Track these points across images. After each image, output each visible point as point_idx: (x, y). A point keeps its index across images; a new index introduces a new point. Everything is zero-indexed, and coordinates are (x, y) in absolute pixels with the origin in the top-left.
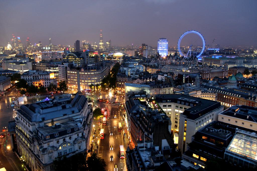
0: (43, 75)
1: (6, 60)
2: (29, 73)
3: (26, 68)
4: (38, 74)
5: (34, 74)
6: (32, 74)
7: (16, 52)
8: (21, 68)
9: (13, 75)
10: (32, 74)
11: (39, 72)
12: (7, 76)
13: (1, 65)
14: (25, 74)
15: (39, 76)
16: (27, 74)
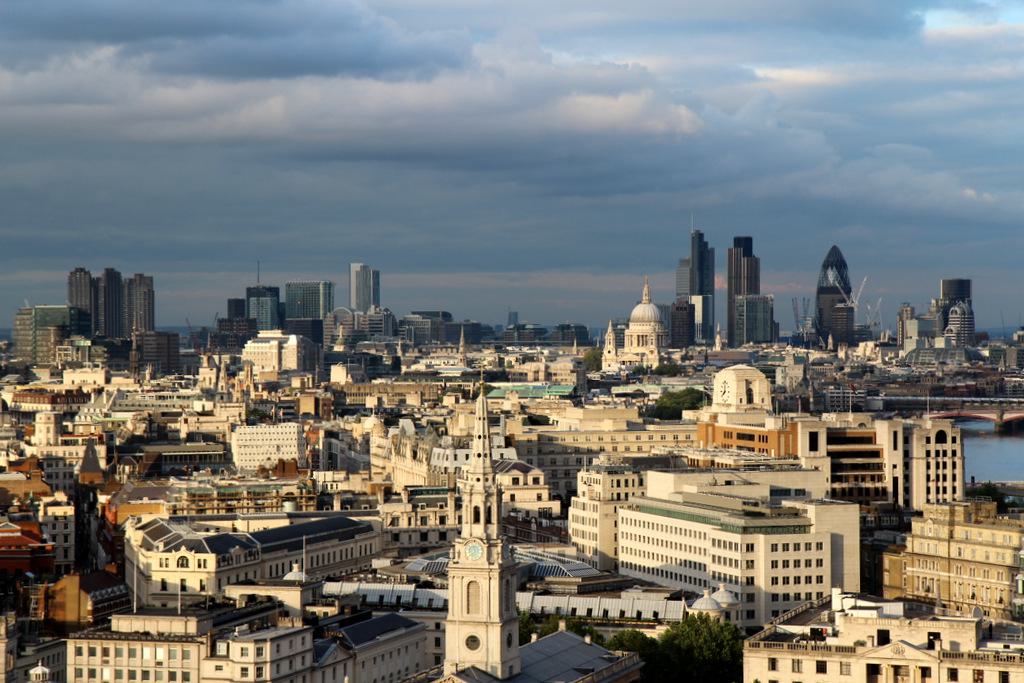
0: (983, 659)
1: (611, 471)
2: (832, 620)
3: (797, 563)
4: (923, 639)
5: (884, 638)
6: (862, 644)
8: (750, 564)
9: (669, 639)
10: (863, 638)
11: (934, 627)
12: (610, 634)
13: (564, 515)
14: (788, 637)
15: (934, 667)
16: (806, 630)
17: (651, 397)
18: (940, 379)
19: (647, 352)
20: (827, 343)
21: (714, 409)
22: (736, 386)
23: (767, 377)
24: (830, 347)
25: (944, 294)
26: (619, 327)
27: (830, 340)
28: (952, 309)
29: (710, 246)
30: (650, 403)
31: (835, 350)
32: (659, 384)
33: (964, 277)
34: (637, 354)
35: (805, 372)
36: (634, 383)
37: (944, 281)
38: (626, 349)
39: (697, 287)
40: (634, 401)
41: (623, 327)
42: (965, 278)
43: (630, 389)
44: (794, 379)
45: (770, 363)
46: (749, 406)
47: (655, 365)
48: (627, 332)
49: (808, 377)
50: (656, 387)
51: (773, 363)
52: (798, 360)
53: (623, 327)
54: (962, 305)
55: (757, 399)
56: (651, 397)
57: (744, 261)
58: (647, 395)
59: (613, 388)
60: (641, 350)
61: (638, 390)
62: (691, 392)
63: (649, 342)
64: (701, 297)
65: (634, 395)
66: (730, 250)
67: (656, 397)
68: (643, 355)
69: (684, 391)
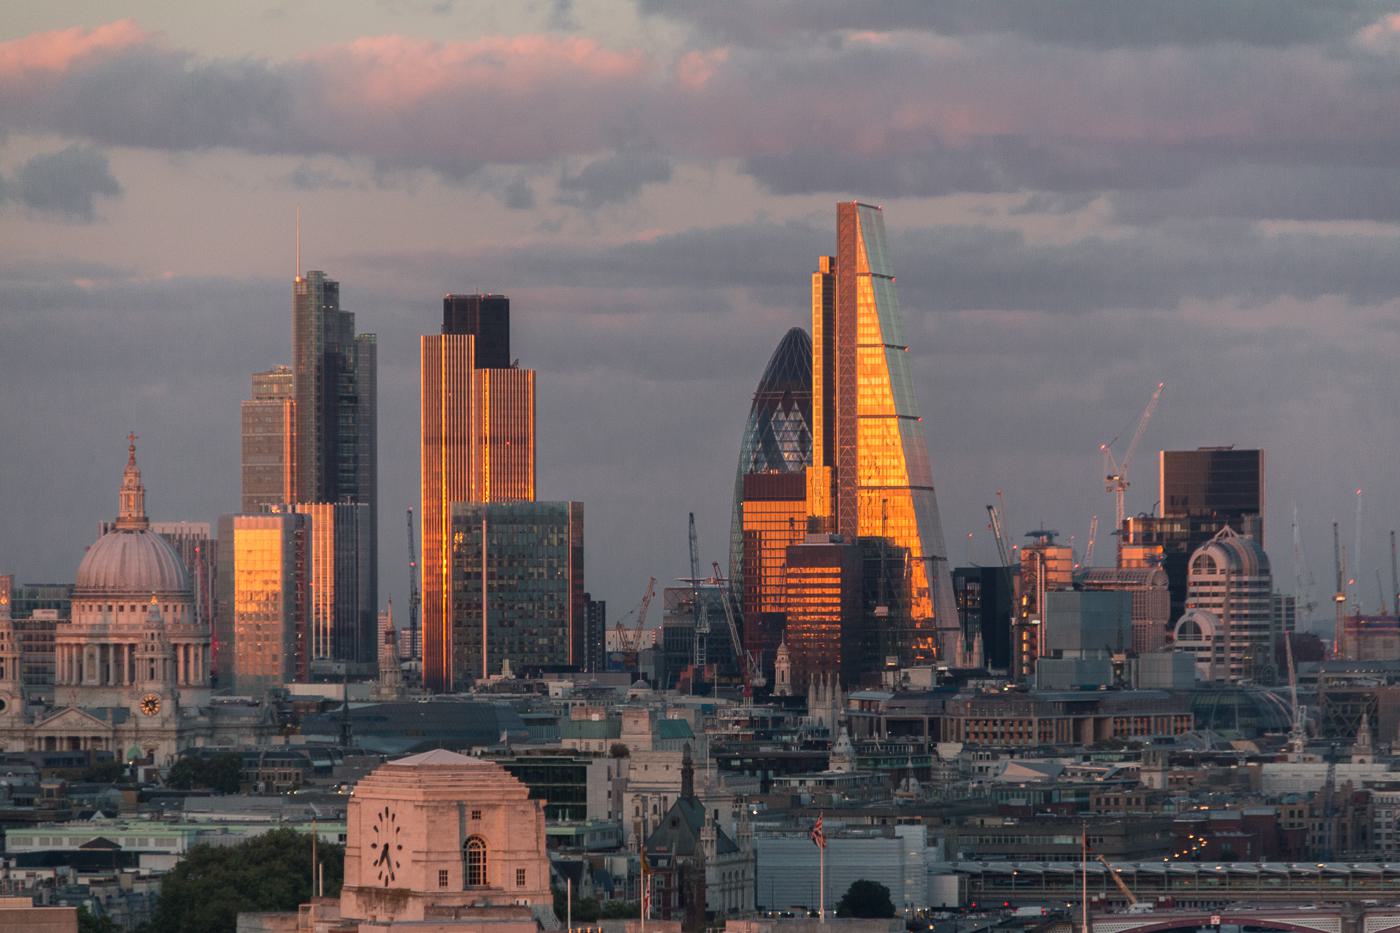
7: (334, 859)
17: (147, 866)
18: (1154, 798)
19: (135, 706)
20: (770, 673)
21: (350, 906)
22: (423, 828)
23: (535, 795)
24: (783, 686)
25: (1171, 501)
26: (39, 615)
27: (782, 665)
28: (1199, 552)
29: (359, 331)
30: (140, 888)
31: (797, 703)
32: (175, 821)
33: (1241, 441)
34: (100, 713)
35: (687, 773)
36: (86, 816)
37: (1166, 454)
38: (60, 698)
39: (312, 473)
40: (84, 881)
41: (52, 615)
42: (1242, 444)
43: (71, 837)
44: (653, 801)
45: (567, 744)
46: (475, 895)
47: (166, 752)
48: (64, 635)
49: (698, 791)
50: (164, 829)
51: (580, 745)
52: (666, 732)
53: (52, 615)
54: (1234, 540)
55: (499, 874)
56: (147, 866)
57: (483, 382)
58: (132, 859)
59: (11, 834)
60: (108, 699)
61: (101, 842)
62: (262, 852)
63: (142, 669)
64: (329, 507)
65: (85, 860)
66: (432, 344)
67: (165, 865)
68: (122, 714)
69: (257, 843)
